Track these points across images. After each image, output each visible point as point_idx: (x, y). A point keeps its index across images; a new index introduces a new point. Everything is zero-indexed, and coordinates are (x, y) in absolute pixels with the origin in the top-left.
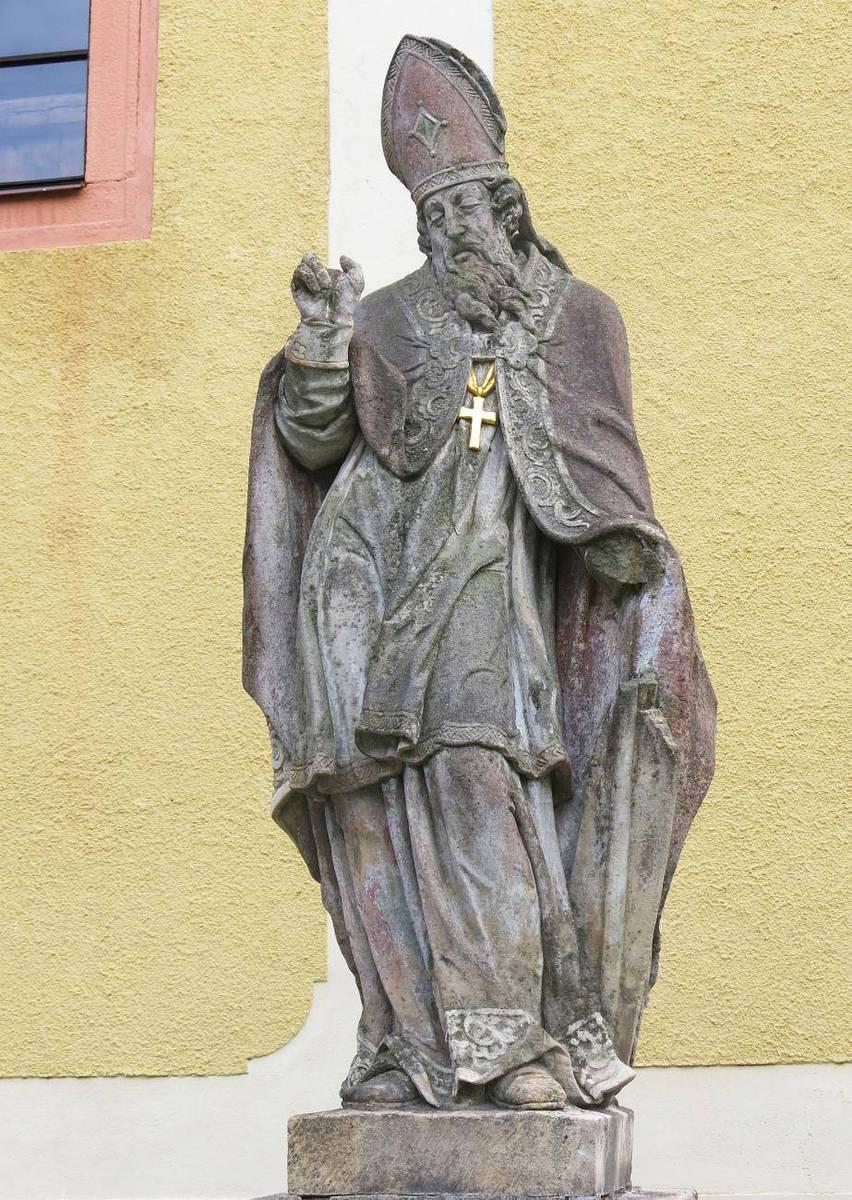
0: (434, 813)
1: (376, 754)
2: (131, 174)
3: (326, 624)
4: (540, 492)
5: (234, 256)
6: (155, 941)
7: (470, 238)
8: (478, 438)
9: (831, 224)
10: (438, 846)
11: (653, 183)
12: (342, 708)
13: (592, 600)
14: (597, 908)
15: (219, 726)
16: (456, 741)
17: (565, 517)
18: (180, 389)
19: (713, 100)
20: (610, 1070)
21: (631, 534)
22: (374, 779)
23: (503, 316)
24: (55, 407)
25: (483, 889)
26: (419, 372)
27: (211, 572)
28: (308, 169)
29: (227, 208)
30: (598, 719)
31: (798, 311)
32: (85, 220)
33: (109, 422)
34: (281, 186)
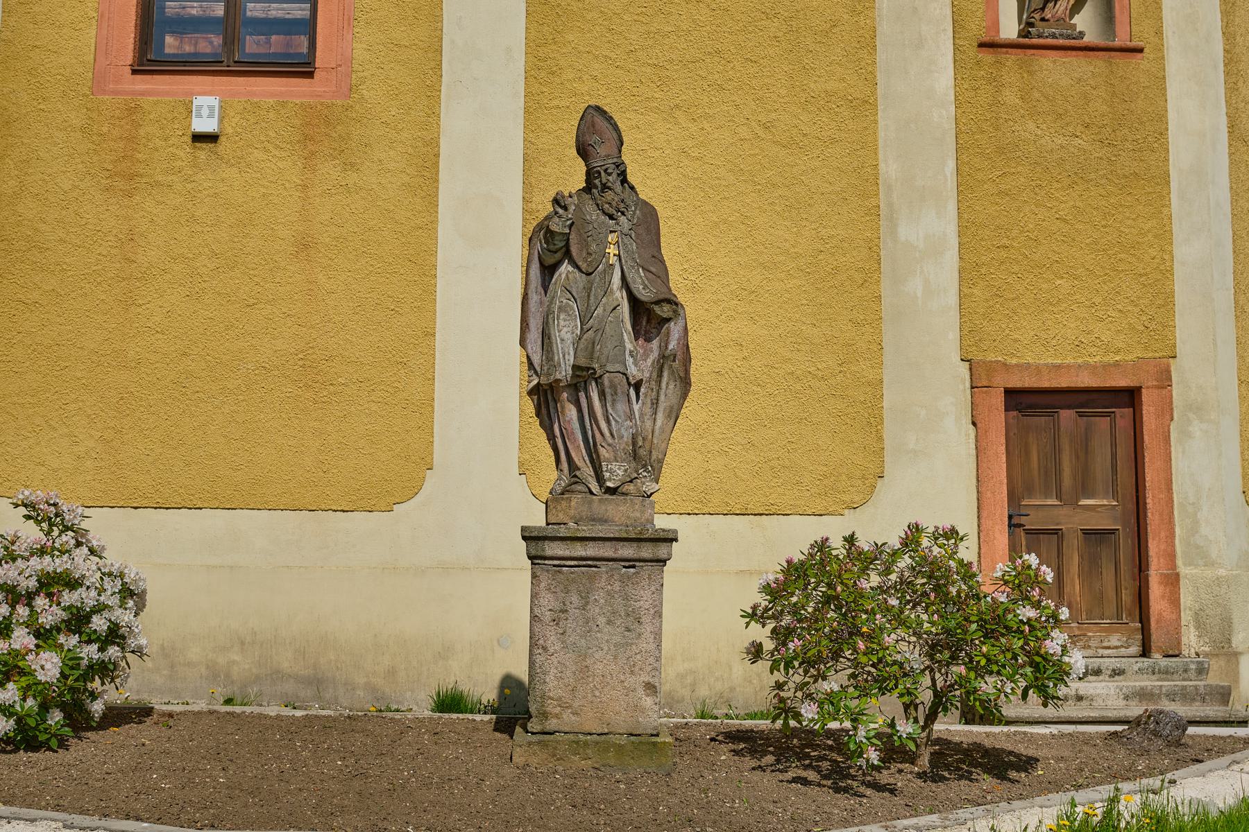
0: (602, 395)
1: (578, 373)
2: (340, 66)
3: (558, 325)
4: (634, 282)
5: (394, 113)
6: (348, 447)
7: (609, 184)
8: (613, 260)
9: (684, 126)
10: (604, 406)
11: (601, 97)
12: (564, 356)
13: (648, 321)
14: (650, 430)
15: (382, 346)
16: (612, 370)
17: (643, 292)
18: (365, 178)
19: (632, 60)
20: (653, 486)
21: (669, 301)
22: (574, 382)
23: (619, 214)
24: (299, 182)
25: (616, 421)
26: (590, 234)
27: (379, 270)
28: (431, 72)
29: (390, 88)
30: (649, 364)
31: (667, 166)
32: (315, 87)
33: (328, 192)
34: (417, 80)
